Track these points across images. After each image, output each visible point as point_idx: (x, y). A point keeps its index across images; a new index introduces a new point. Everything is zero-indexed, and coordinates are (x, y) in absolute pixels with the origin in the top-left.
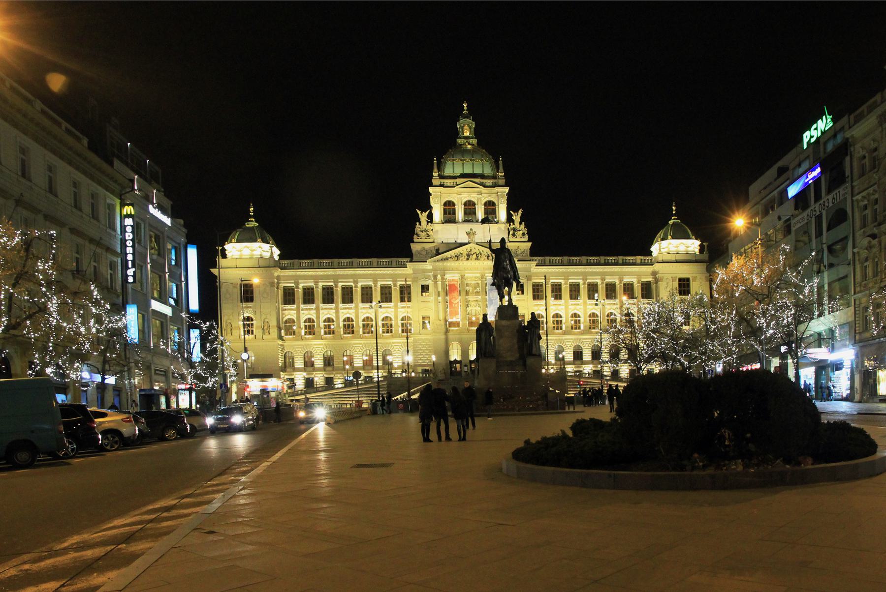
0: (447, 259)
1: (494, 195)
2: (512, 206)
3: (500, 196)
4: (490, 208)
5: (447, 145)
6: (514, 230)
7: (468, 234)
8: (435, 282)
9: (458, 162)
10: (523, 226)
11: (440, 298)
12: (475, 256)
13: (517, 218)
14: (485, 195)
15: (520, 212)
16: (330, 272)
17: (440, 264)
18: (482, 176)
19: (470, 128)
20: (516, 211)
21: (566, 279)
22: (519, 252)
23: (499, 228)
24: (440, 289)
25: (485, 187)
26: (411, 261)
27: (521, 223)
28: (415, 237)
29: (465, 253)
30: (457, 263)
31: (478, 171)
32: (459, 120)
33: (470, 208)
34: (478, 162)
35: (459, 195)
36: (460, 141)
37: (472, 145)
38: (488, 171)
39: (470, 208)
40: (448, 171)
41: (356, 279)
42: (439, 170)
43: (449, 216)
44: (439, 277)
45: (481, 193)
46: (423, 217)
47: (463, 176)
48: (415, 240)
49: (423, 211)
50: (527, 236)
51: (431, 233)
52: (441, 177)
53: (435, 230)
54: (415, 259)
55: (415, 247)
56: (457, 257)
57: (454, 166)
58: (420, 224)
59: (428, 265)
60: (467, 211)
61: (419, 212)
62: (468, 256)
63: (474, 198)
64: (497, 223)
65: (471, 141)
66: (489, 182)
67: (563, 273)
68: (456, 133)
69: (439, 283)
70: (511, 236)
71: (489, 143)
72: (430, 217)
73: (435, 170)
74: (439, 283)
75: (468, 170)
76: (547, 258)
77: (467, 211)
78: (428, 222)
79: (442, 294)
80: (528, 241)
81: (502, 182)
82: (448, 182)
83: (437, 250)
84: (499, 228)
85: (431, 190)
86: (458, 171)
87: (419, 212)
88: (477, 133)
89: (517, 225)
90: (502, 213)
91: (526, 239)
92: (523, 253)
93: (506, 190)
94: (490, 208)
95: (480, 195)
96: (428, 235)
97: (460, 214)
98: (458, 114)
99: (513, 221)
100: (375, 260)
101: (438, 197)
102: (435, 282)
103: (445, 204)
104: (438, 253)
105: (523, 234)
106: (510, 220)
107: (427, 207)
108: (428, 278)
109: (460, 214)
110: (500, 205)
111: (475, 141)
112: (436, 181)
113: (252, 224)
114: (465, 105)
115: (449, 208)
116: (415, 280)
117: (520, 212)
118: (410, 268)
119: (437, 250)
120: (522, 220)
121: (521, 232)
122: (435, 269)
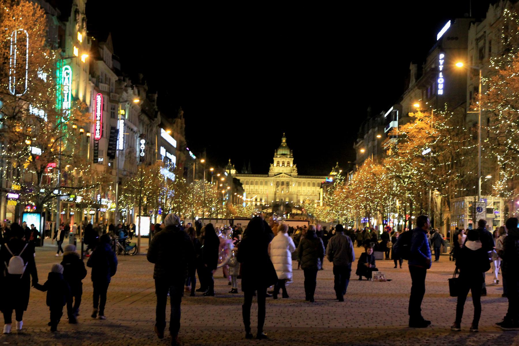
2: (294, 163)
3: (291, 160)
4: (288, 163)
5: (278, 145)
13: (295, 166)
26: (268, 176)
31: (286, 153)
33: (283, 163)
35: (281, 160)
38: (288, 153)
39: (283, 163)
40: (278, 153)
46: (272, 165)
53: (275, 168)
55: (270, 173)
56: (279, 177)
57: (280, 151)
59: (272, 178)
60: (283, 164)
71: (290, 146)
75: (284, 153)
77: (283, 164)
85: (274, 158)
86: (281, 153)
90: (291, 165)
93: (293, 159)
94: (288, 163)
95: (286, 160)
97: (281, 165)
101: (276, 160)
107: (273, 163)
115: (278, 163)
120: (296, 167)
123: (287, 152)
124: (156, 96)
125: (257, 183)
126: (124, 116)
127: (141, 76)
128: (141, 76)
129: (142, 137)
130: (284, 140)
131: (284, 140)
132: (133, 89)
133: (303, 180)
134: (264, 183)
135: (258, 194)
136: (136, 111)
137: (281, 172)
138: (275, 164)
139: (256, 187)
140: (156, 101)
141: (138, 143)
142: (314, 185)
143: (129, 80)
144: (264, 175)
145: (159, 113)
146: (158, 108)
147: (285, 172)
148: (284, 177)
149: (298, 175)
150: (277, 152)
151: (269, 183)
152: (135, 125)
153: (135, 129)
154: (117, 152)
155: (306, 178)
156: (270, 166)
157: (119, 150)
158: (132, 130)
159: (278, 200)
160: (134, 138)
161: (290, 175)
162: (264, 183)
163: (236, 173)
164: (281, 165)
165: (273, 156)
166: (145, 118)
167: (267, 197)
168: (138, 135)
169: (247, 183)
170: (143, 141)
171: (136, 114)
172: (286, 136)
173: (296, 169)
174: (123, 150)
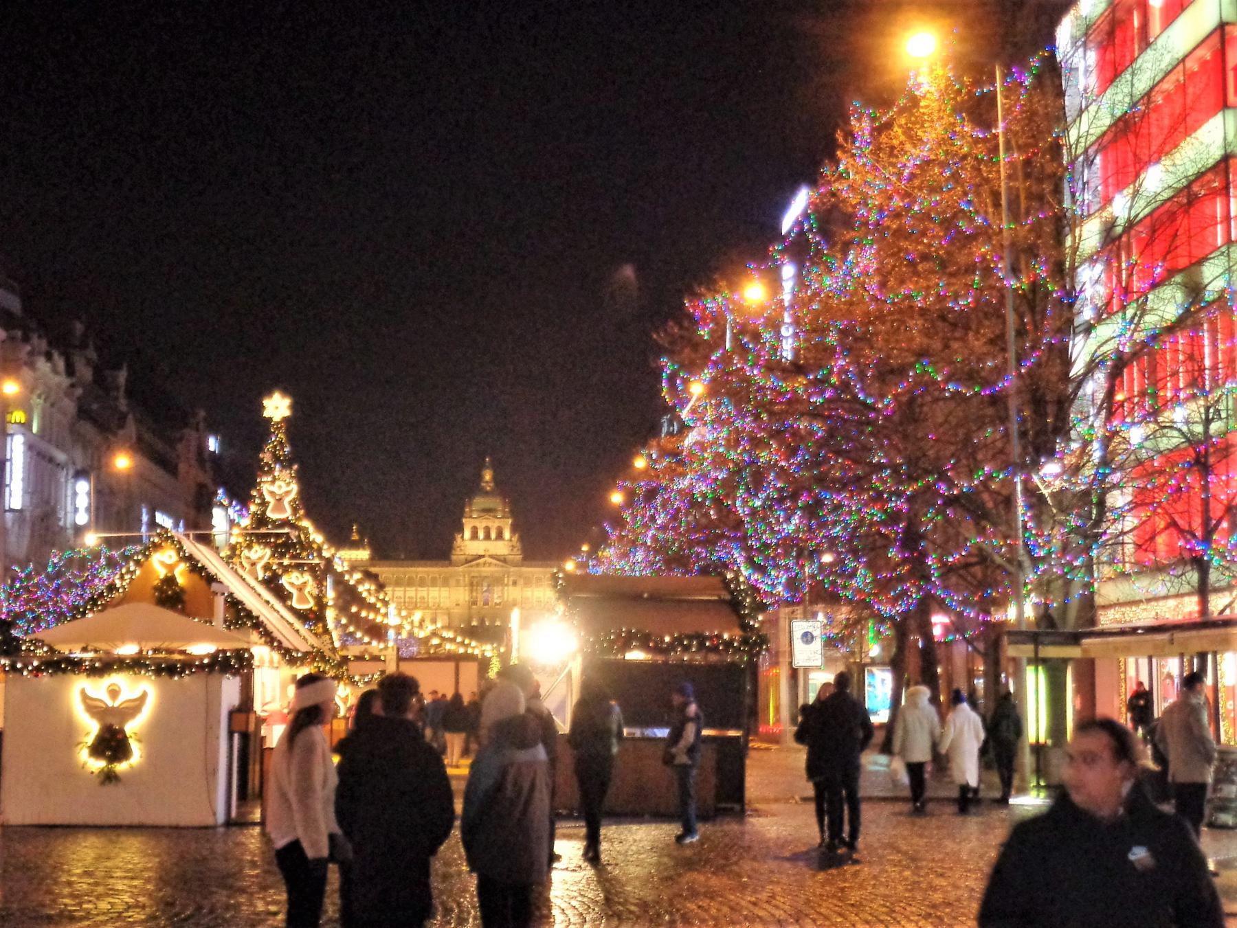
5: (473, 487)
13: (515, 539)
31: (492, 506)
35: (481, 525)
43: (474, 536)
46: (458, 537)
53: (467, 544)
55: (454, 558)
56: (478, 565)
57: (479, 502)
59: (461, 569)
60: (485, 535)
63: (490, 524)
68: (480, 477)
71: (503, 487)
77: (485, 535)
85: (464, 520)
86: (482, 506)
90: (507, 534)
93: (510, 521)
95: (494, 524)
97: (481, 535)
104: (467, 561)
107: (461, 529)
113: (355, 537)
118: (450, 569)
123: (495, 502)
124: (122, 376)
125: (422, 583)
126: (27, 425)
127: (79, 328)
128: (79, 328)
129: (80, 474)
130: (488, 476)
131: (488, 476)
132: (49, 357)
134: (439, 582)
135: (427, 608)
136: (65, 414)
138: (467, 534)
139: (422, 592)
140: (122, 389)
141: (69, 493)
143: (40, 337)
144: (440, 563)
145: (130, 416)
146: (128, 405)
147: (493, 552)
148: (490, 564)
149: (525, 559)
150: (470, 505)
151: (452, 582)
152: (60, 446)
153: (61, 457)
154: (9, 516)
156: (454, 539)
157: (11, 510)
158: (51, 460)
159: (474, 623)
160: (58, 481)
162: (439, 582)
163: (372, 558)
164: (481, 535)
165: (461, 514)
166: (87, 428)
167: (449, 615)
168: (71, 472)
169: (398, 583)
170: (83, 487)
171: (65, 421)
173: (518, 545)
174: (21, 511)
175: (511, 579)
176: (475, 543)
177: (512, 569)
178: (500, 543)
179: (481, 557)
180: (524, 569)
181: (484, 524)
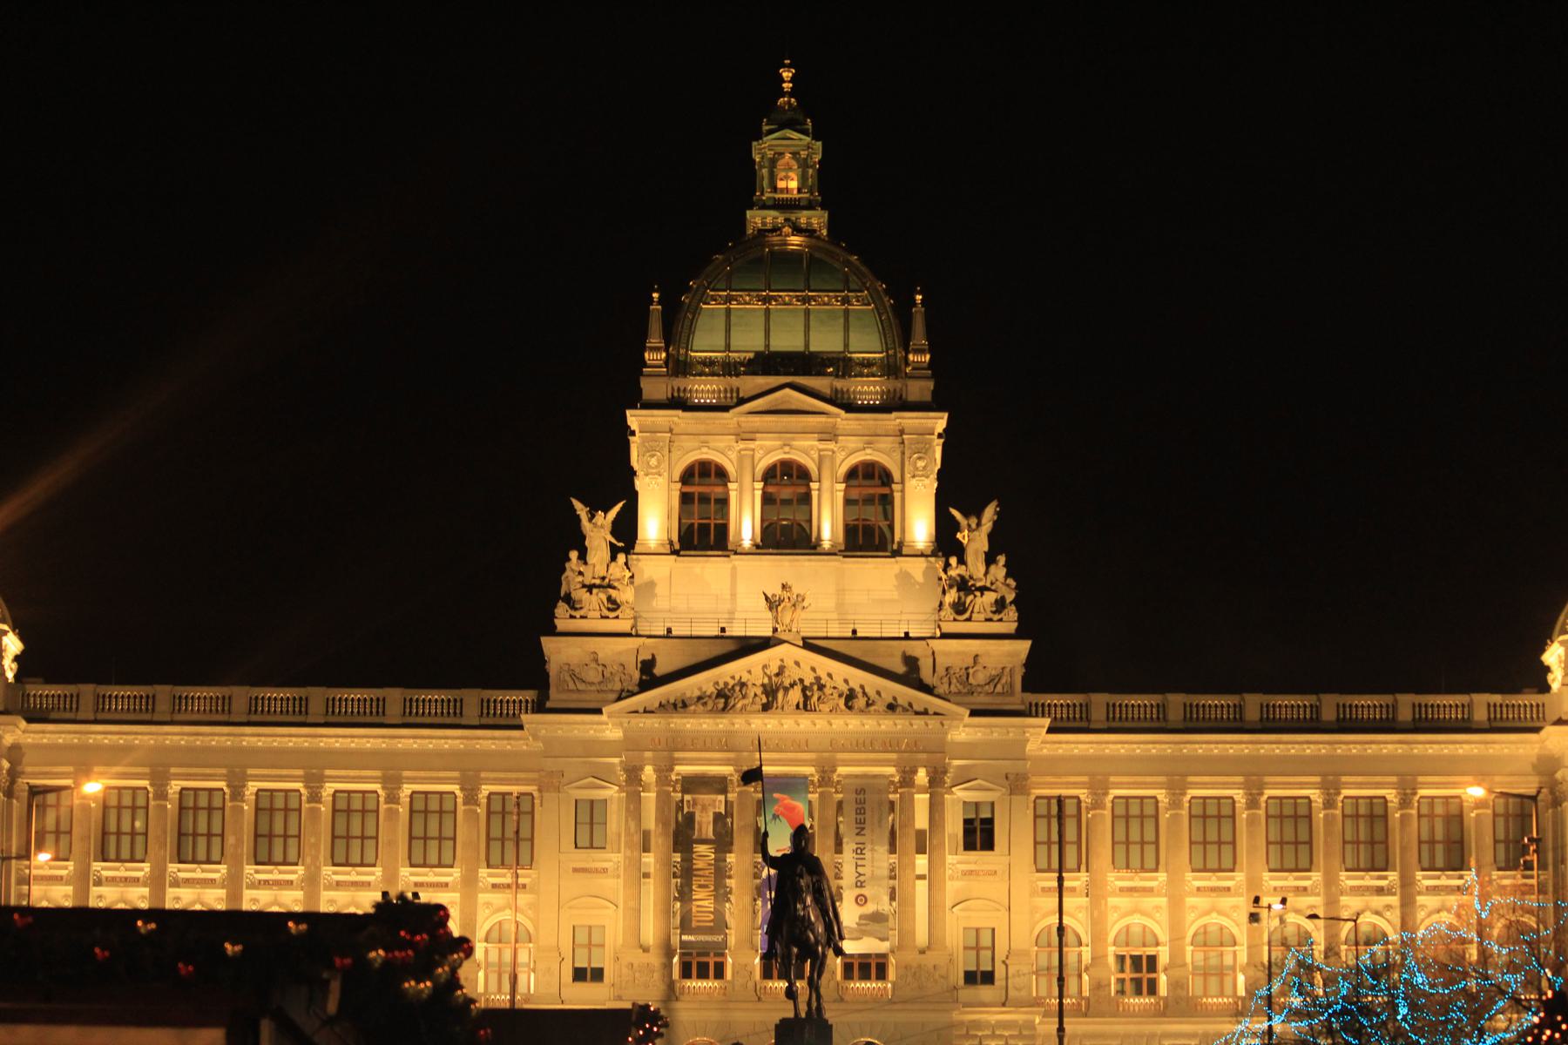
0: (679, 706)
1: (887, 443)
5: (705, 237)
6: (963, 585)
7: (772, 604)
8: (634, 801)
9: (748, 307)
10: (999, 571)
11: (649, 860)
12: (795, 695)
13: (975, 538)
14: (853, 442)
15: (990, 513)
16: (218, 737)
17: (653, 723)
18: (843, 365)
19: (804, 165)
20: (974, 510)
21: (1177, 788)
22: (979, 678)
23: (904, 577)
24: (650, 821)
25: (850, 407)
26: (540, 707)
27: (990, 559)
28: (561, 609)
29: (758, 678)
30: (722, 723)
31: (826, 341)
32: (759, 136)
34: (828, 303)
36: (757, 219)
37: (808, 232)
38: (867, 344)
40: (706, 343)
41: (315, 768)
42: (669, 338)
44: (649, 773)
45: (830, 435)
46: (598, 530)
47: (767, 363)
48: (562, 624)
49: (597, 505)
50: (1011, 614)
51: (625, 595)
52: (680, 367)
54: (556, 697)
56: (725, 699)
57: (732, 324)
58: (583, 557)
59: (609, 727)
61: (581, 509)
62: (771, 692)
63: (804, 450)
64: (897, 553)
65: (803, 217)
66: (868, 388)
67: (1161, 759)
68: (744, 184)
69: (650, 797)
70: (948, 612)
72: (626, 533)
73: (655, 340)
74: (650, 797)
75: (787, 340)
76: (1099, 701)
78: (614, 553)
79: (660, 842)
80: (1018, 635)
81: (920, 389)
82: (704, 388)
83: (647, 666)
84: (904, 577)
86: (748, 341)
87: (581, 509)
88: (830, 185)
89: (975, 567)
91: (1011, 627)
92: (994, 680)
93: (940, 422)
95: (832, 447)
96: (614, 605)
98: (757, 111)
99: (959, 551)
100: (394, 697)
102: (634, 801)
103: (687, 477)
104: (649, 678)
105: (1000, 605)
106: (946, 543)
107: (618, 488)
108: (603, 776)
109: (746, 522)
110: (911, 483)
111: (817, 219)
112: (653, 388)
114: (787, 75)
116: (551, 782)
117: (990, 513)
119: (647, 666)
121: (990, 597)
122: (631, 744)
133: (1111, 761)
137: (761, 628)
138: (656, 519)
142: (1293, 840)
147: (820, 618)
149: (1041, 675)
155: (1159, 725)
161: (911, 675)
172: (816, 111)
175: (958, 798)
176: (709, 569)
177: (964, 731)
178: (874, 573)
179: (750, 646)
180: (1036, 736)
181: (768, 452)
